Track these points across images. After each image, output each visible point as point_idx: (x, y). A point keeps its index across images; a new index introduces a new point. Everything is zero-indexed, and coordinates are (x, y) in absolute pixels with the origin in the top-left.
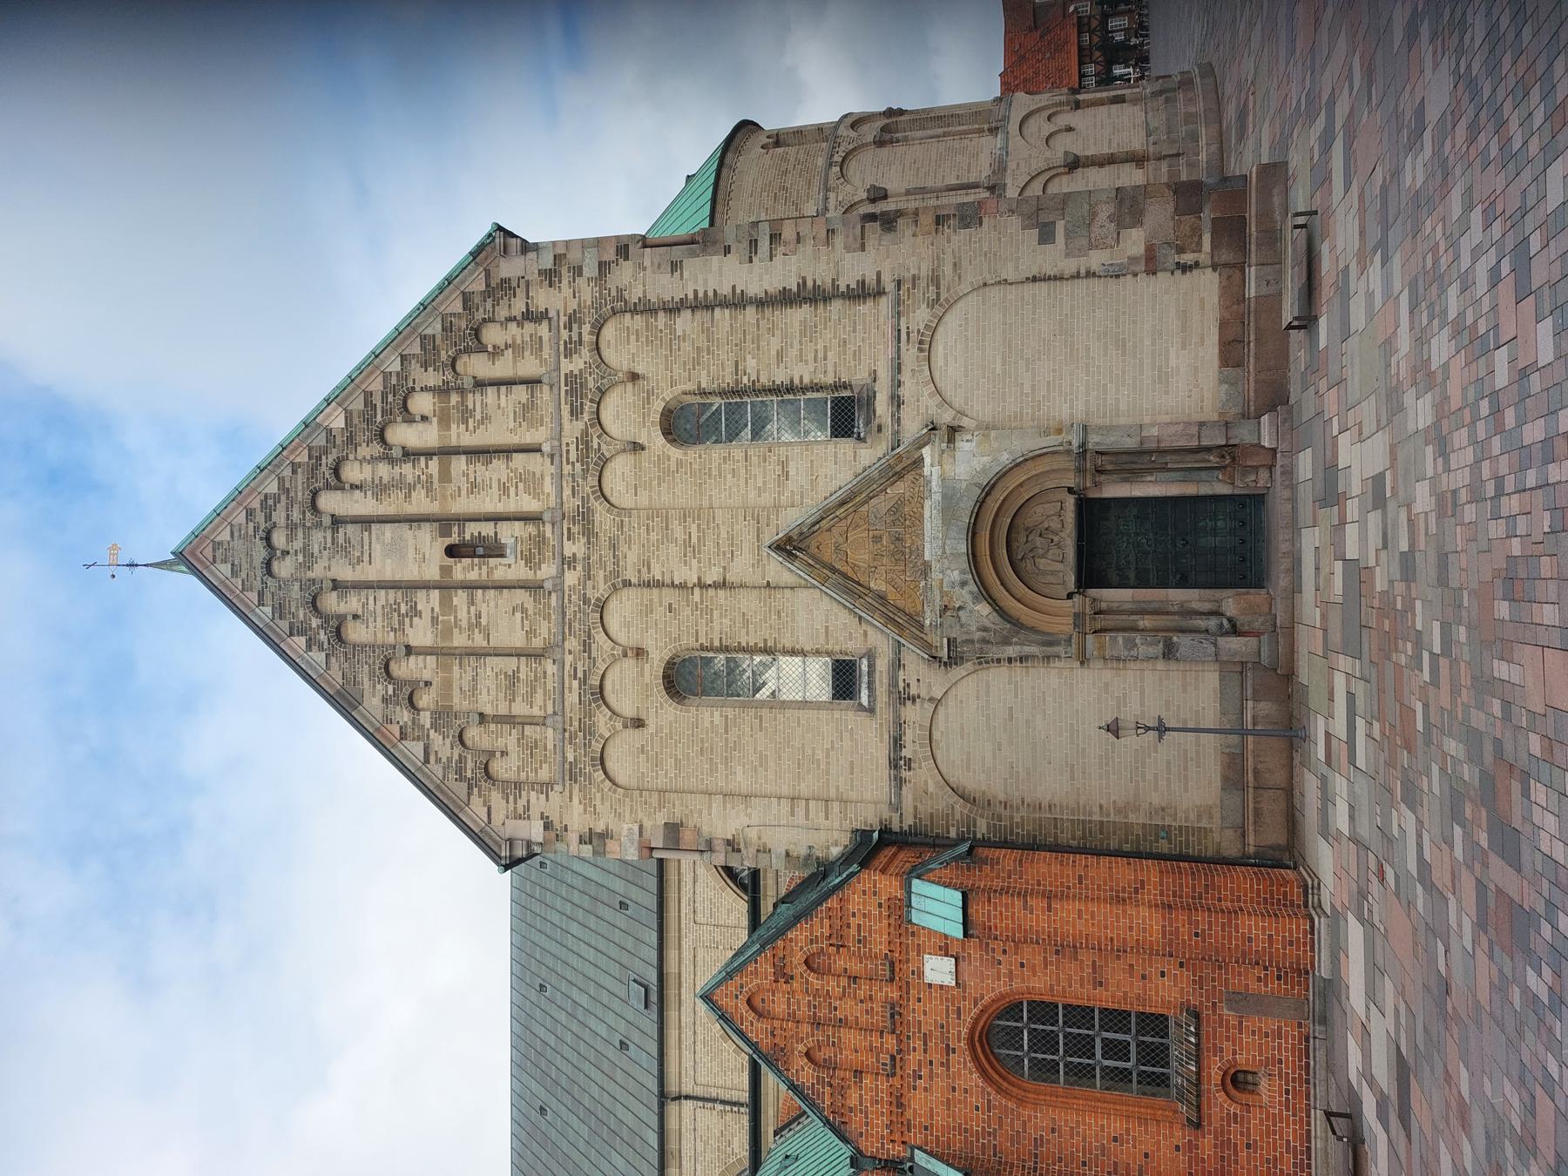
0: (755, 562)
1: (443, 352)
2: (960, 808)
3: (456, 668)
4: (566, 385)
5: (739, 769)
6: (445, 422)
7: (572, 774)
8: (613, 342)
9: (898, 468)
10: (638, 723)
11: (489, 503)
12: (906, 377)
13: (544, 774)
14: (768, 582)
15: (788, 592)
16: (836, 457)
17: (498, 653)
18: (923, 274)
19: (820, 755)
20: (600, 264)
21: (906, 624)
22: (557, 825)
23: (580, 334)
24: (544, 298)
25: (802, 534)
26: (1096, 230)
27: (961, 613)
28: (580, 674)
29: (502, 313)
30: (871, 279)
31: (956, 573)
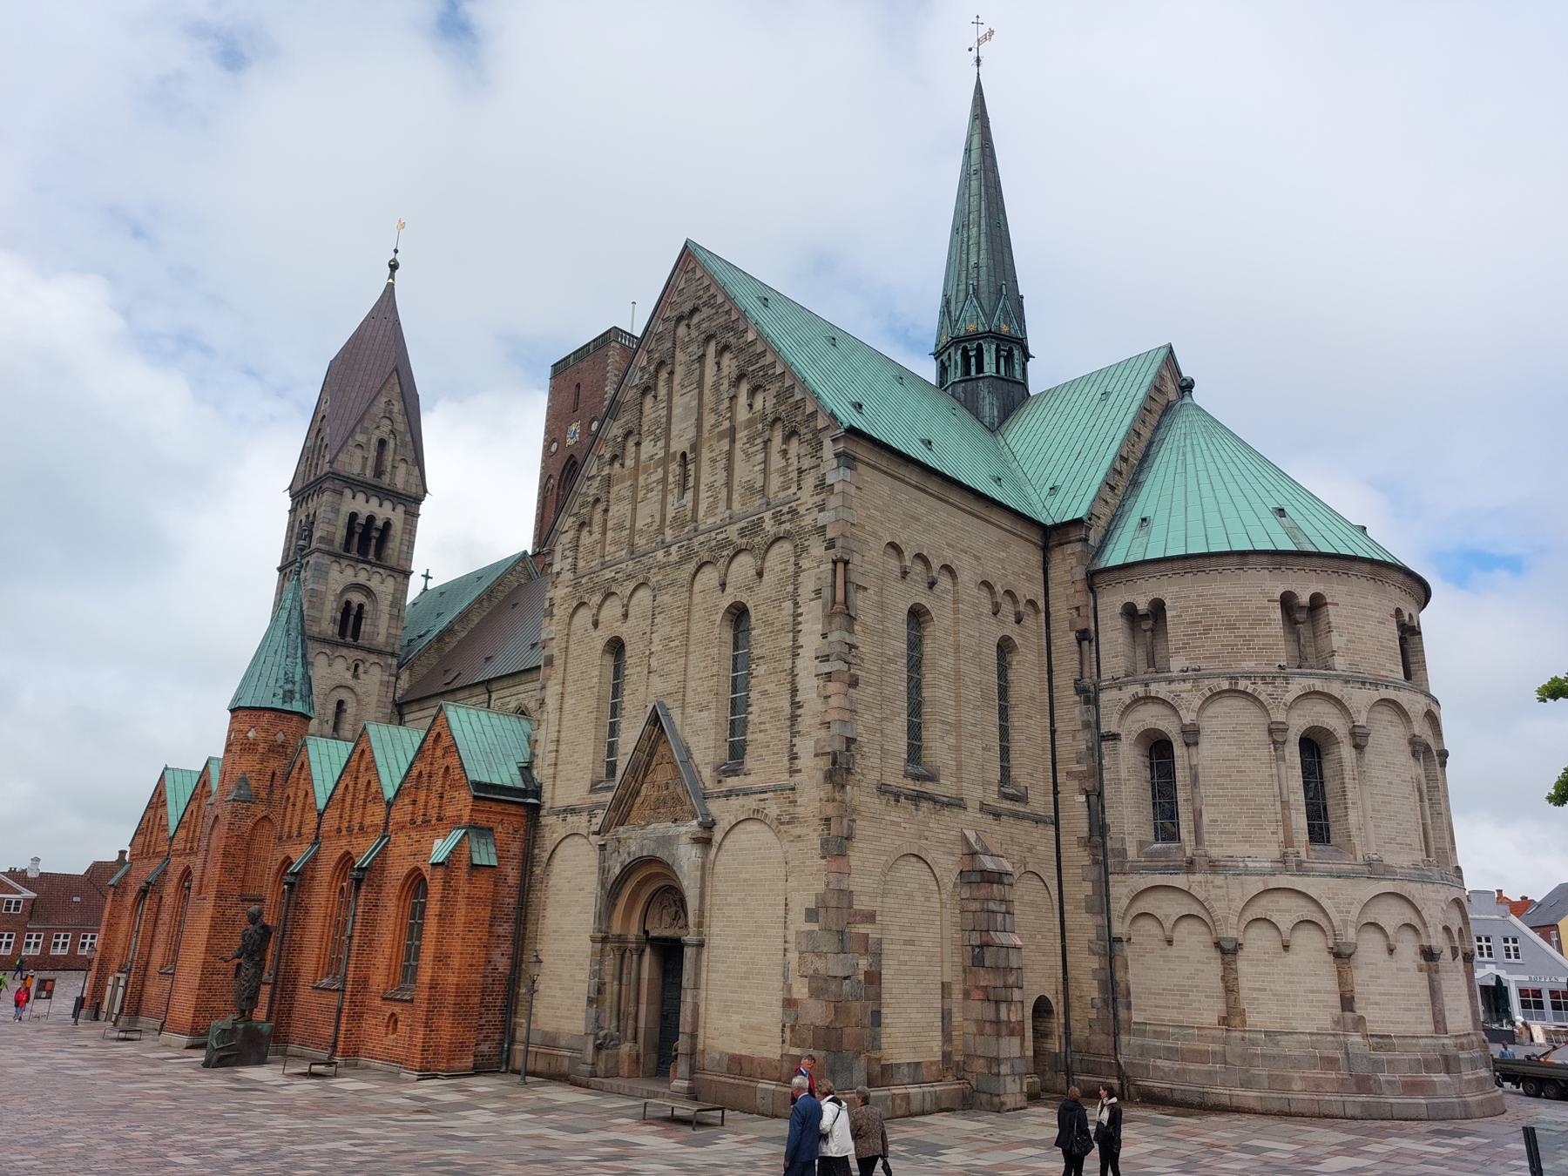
1: (783, 408)
2: (546, 855)
3: (629, 483)
4: (758, 519)
5: (573, 701)
6: (751, 423)
7: (577, 585)
8: (783, 550)
10: (596, 624)
11: (705, 479)
12: (741, 800)
13: (581, 564)
17: (634, 510)
18: (799, 810)
19: (576, 756)
20: (825, 526)
22: (560, 579)
23: (784, 522)
24: (810, 481)
26: (810, 957)
28: (618, 576)
29: (805, 449)
30: (799, 764)
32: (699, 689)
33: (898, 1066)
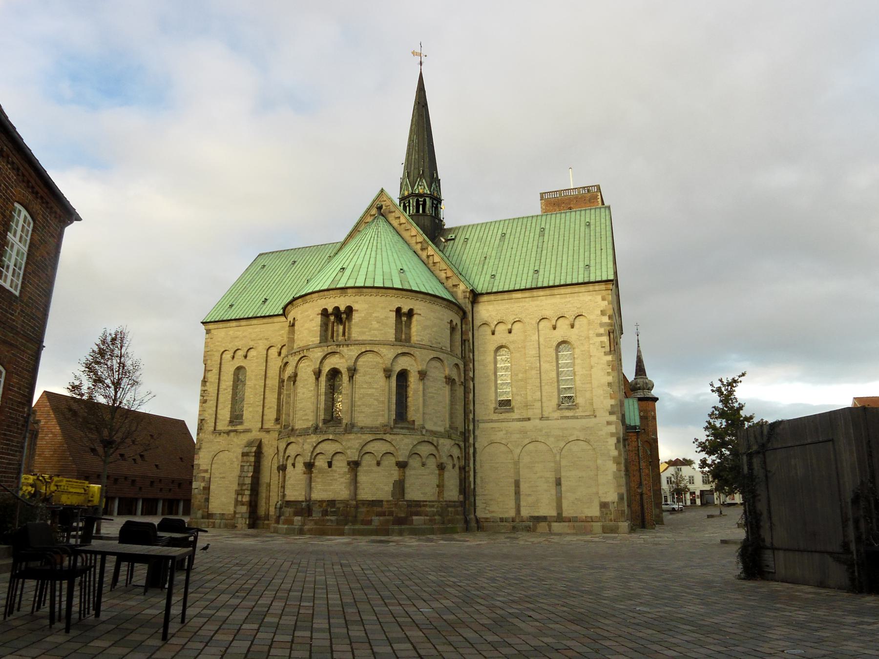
33: (215, 514)
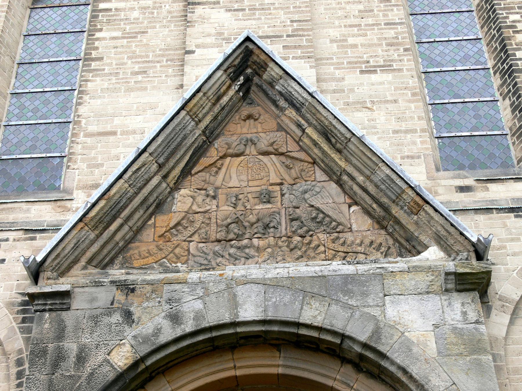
0: (226, 35)
9: (395, 210)
14: (192, 52)
15: (174, 81)
16: (407, 132)
21: (106, 235)
25: (271, 85)
27: (117, 318)
31: (198, 305)
32: (351, 41)
